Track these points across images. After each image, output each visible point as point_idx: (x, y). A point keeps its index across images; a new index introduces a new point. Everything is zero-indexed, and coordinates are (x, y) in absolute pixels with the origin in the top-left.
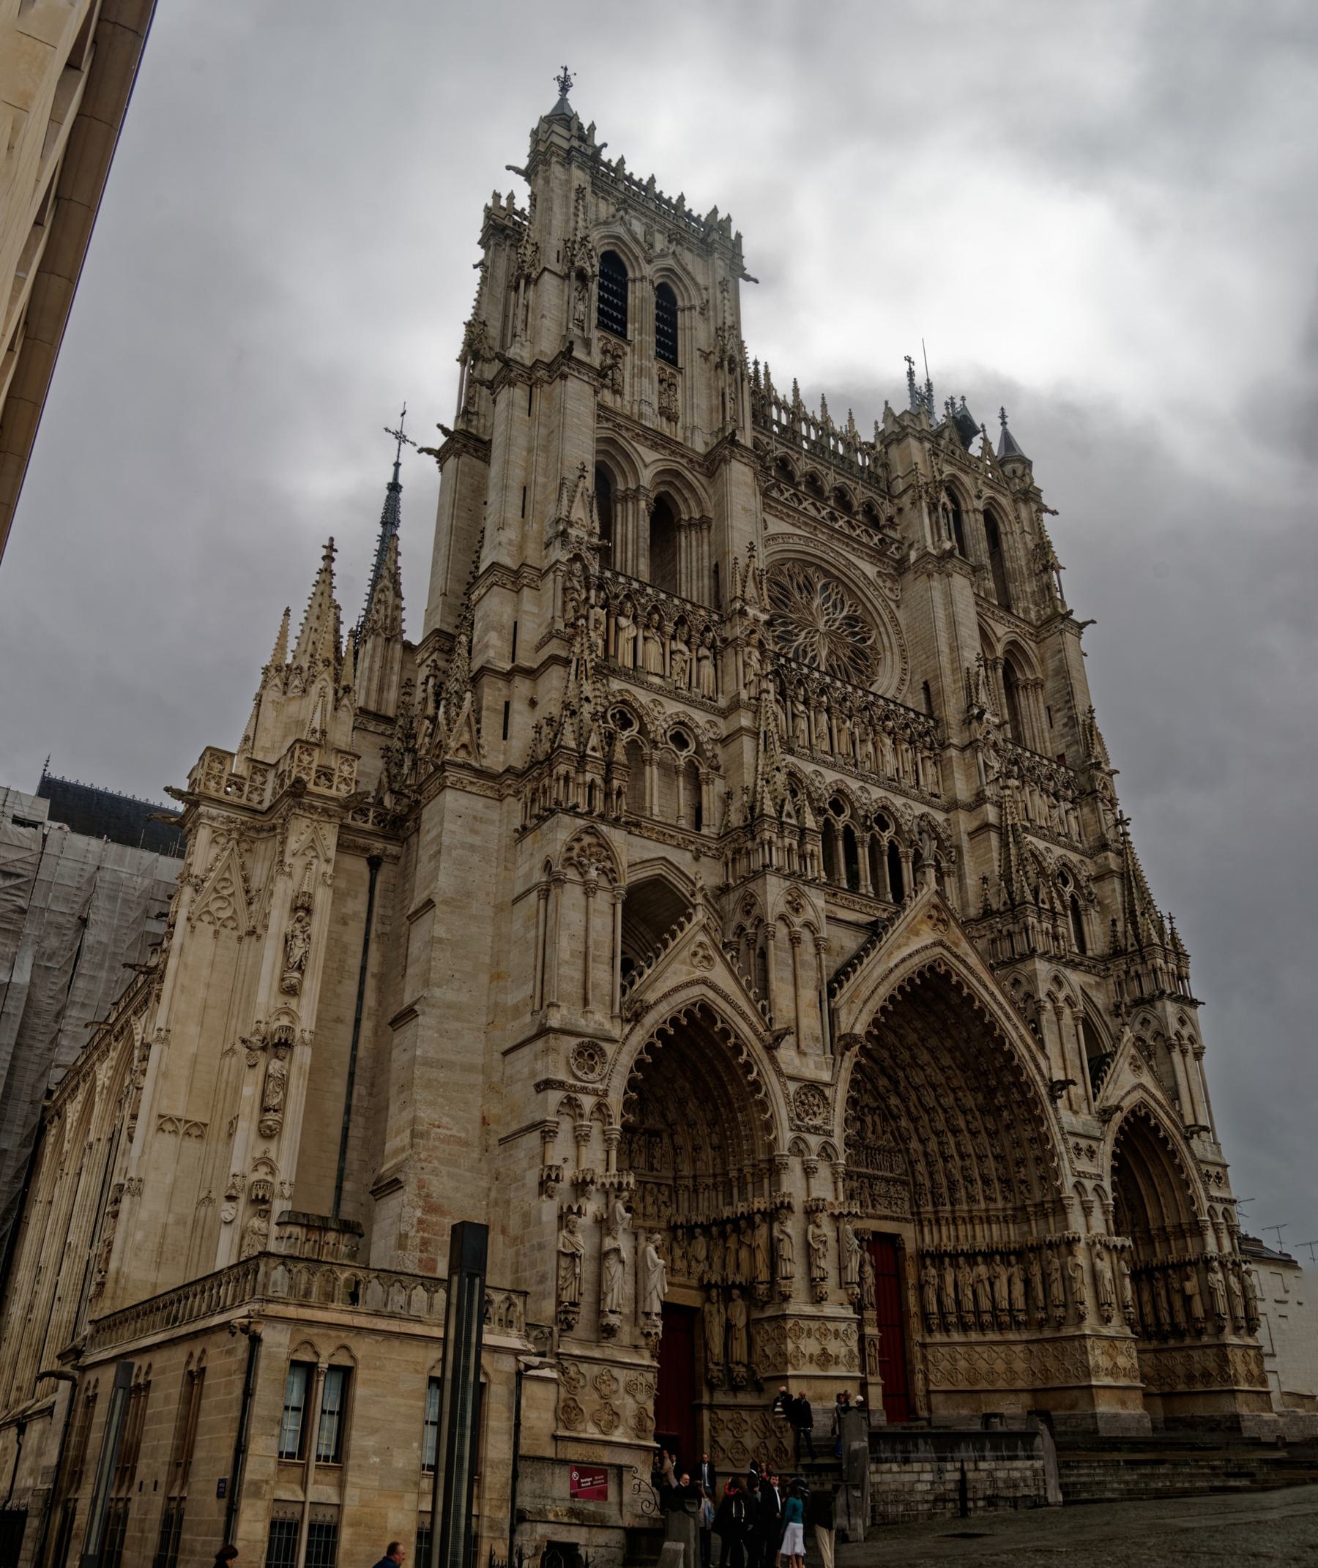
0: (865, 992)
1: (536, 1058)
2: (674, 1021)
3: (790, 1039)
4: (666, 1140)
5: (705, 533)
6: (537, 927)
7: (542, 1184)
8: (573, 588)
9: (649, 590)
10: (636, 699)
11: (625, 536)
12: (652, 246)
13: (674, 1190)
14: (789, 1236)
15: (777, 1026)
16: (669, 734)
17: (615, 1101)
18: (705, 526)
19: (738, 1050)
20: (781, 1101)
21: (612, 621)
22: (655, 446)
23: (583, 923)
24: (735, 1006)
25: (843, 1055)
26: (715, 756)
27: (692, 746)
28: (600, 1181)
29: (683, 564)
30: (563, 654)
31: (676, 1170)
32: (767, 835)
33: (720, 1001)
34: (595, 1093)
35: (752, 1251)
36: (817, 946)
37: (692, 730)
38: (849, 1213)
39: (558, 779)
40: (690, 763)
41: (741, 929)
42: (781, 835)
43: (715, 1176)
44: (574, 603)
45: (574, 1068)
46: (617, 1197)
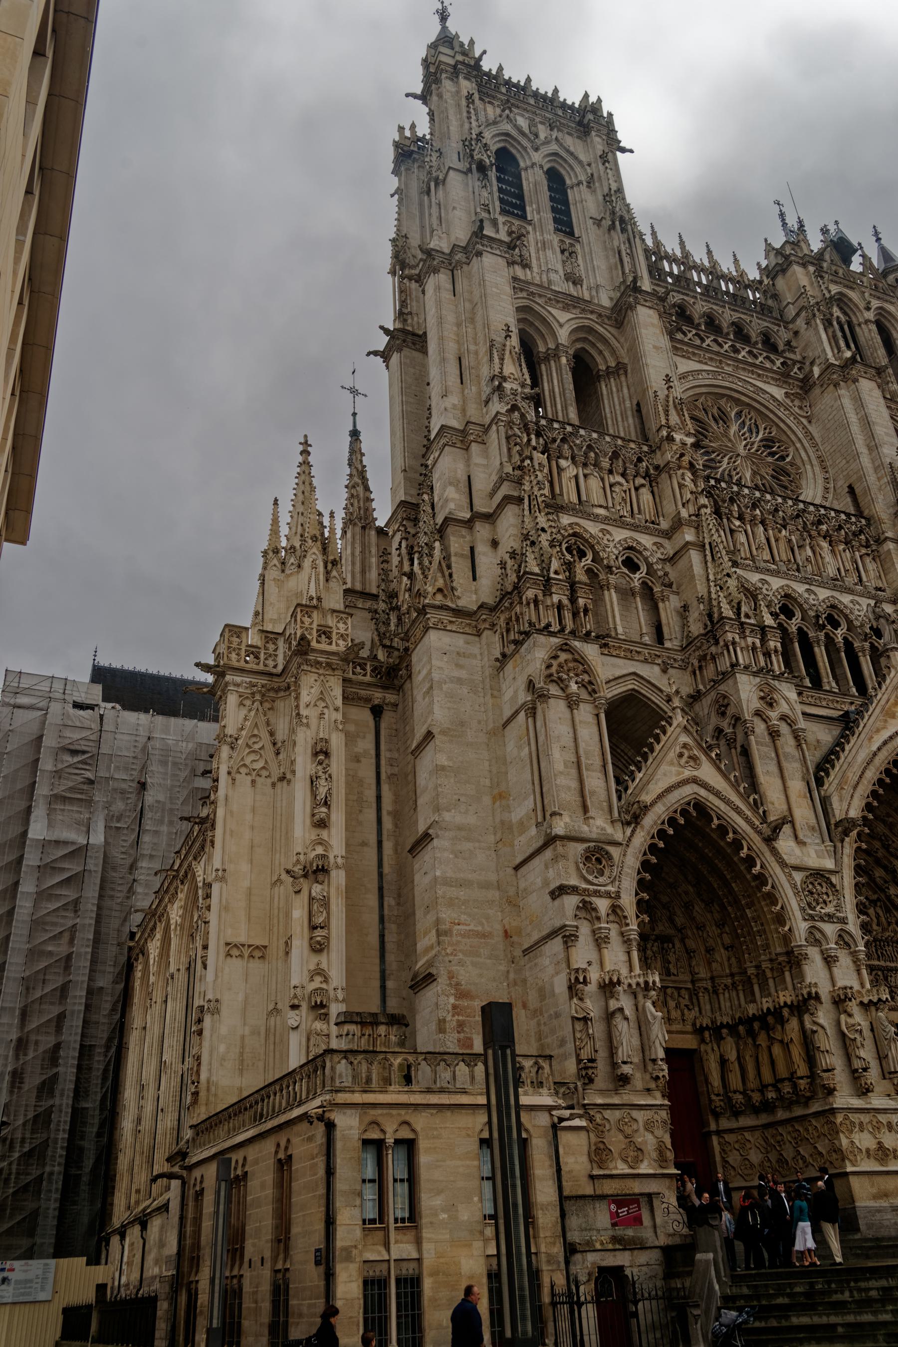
0: (852, 777)
1: (547, 867)
2: (672, 821)
3: (787, 829)
4: (678, 945)
5: (623, 378)
6: (529, 744)
7: (570, 988)
8: (515, 435)
9: (582, 432)
10: (586, 531)
11: (552, 391)
12: (536, 136)
13: (694, 994)
14: (822, 1027)
15: (771, 818)
16: (620, 560)
17: (628, 902)
18: (621, 372)
19: (737, 845)
20: (790, 893)
21: (554, 463)
22: (566, 308)
23: (571, 735)
24: (728, 802)
25: (842, 841)
26: (666, 574)
27: (644, 568)
28: (626, 982)
29: (607, 410)
30: (516, 494)
31: (693, 973)
32: (729, 636)
33: (712, 798)
34: (608, 895)
35: (786, 1046)
36: (797, 738)
37: (640, 553)
38: (880, 1000)
39: (528, 604)
40: (644, 584)
41: (719, 731)
42: (744, 637)
43: (732, 975)
44: (518, 448)
45: (584, 872)
46: (645, 997)
